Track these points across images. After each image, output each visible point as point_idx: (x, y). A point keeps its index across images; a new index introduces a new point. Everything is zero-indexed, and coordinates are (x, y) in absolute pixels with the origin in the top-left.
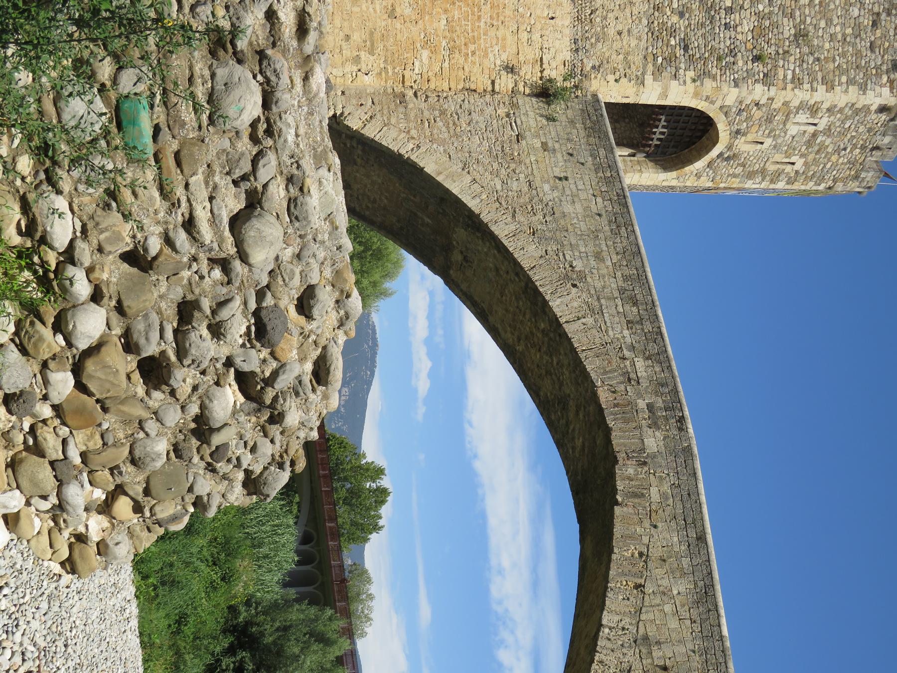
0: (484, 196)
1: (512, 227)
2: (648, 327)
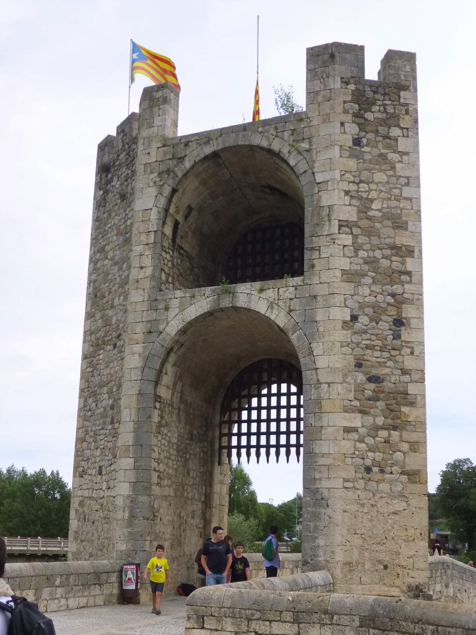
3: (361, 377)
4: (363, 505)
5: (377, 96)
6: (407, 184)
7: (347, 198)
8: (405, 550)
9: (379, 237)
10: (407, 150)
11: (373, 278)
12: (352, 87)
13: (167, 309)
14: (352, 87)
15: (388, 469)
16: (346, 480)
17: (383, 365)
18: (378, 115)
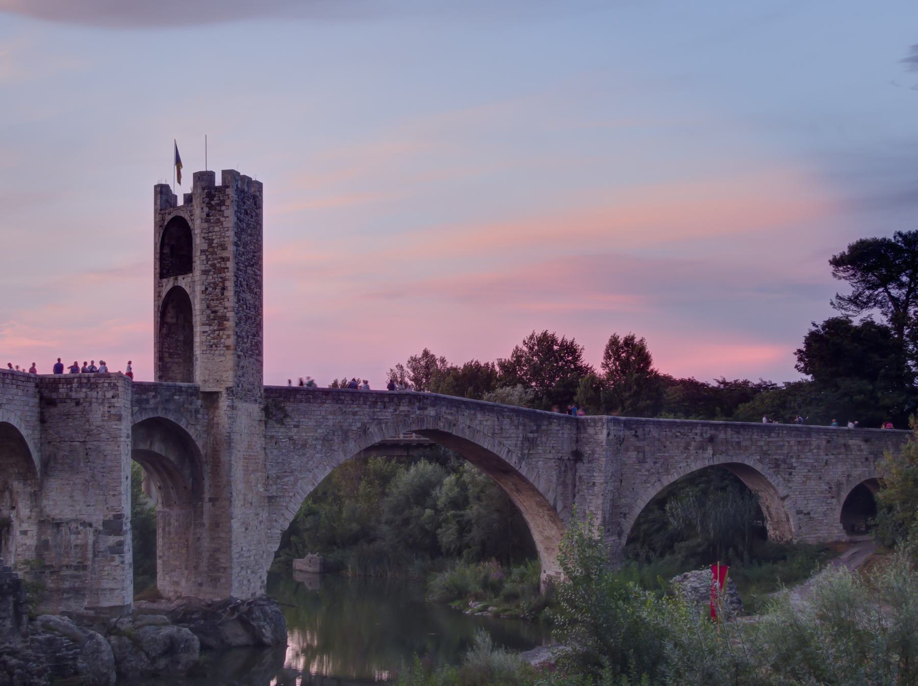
0: (325, 463)
1: (341, 453)
2: (386, 400)
4: (209, 359)
5: (216, 193)
6: (227, 231)
8: (225, 375)
12: (206, 191)
13: (162, 286)
14: (206, 191)
16: (203, 351)
17: (217, 306)
18: (216, 202)
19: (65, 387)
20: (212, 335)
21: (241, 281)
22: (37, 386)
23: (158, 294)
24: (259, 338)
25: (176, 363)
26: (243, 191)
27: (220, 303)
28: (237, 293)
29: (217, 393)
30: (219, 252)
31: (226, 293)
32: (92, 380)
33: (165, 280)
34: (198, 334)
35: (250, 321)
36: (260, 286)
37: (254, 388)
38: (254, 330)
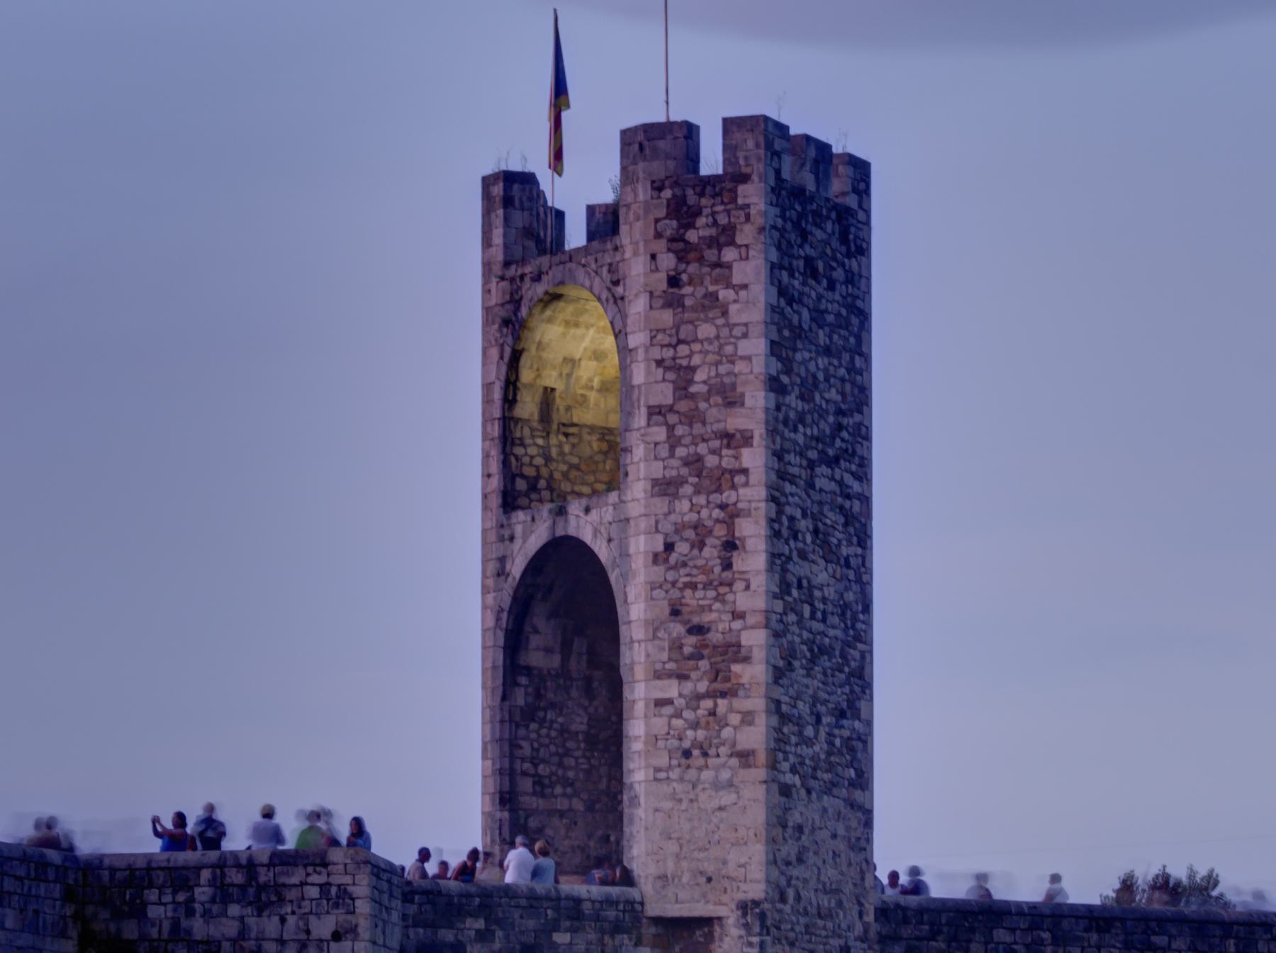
3: (678, 629)
5: (704, 201)
6: (745, 336)
7: (660, 371)
8: (735, 857)
9: (704, 423)
10: (745, 281)
11: (695, 485)
12: (667, 193)
13: (512, 539)
14: (667, 193)
15: (712, 752)
16: (657, 770)
18: (702, 233)
19: (168, 898)
20: (688, 714)
21: (792, 519)
22: (69, 896)
23: (497, 568)
24: (857, 724)
25: (562, 814)
26: (798, 193)
27: (720, 598)
28: (778, 562)
29: (707, 922)
30: (713, 413)
31: (738, 564)
32: (264, 876)
33: (520, 516)
34: (640, 708)
35: (825, 661)
36: (863, 538)
37: (840, 904)
38: (840, 697)
